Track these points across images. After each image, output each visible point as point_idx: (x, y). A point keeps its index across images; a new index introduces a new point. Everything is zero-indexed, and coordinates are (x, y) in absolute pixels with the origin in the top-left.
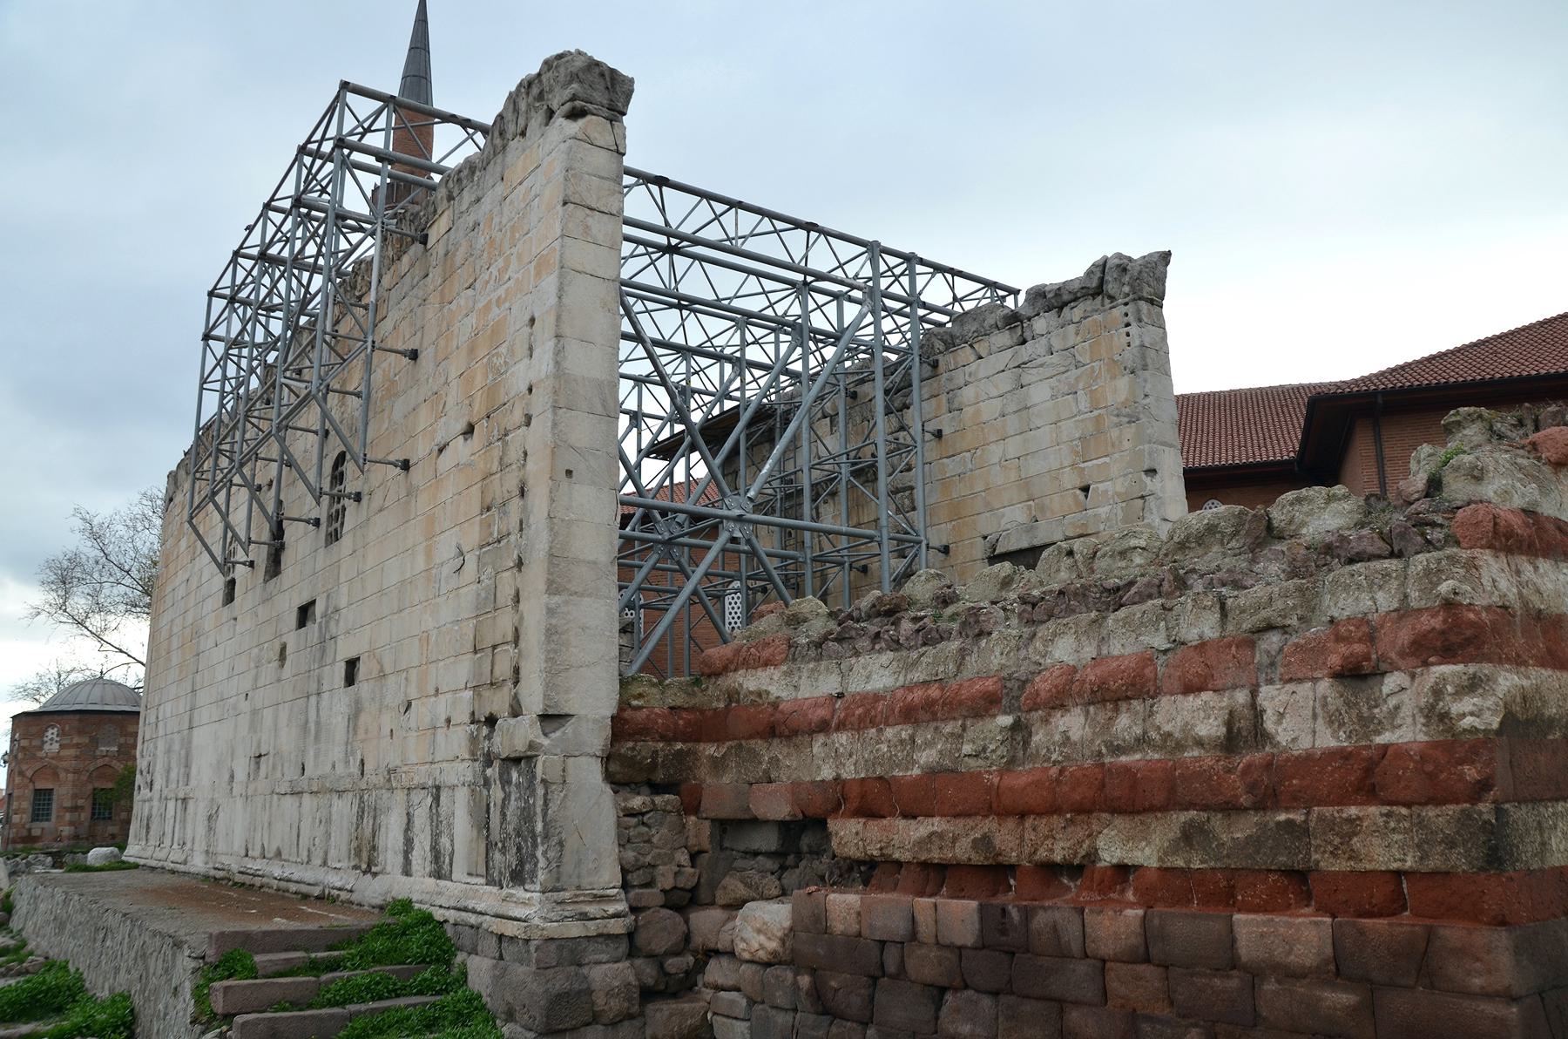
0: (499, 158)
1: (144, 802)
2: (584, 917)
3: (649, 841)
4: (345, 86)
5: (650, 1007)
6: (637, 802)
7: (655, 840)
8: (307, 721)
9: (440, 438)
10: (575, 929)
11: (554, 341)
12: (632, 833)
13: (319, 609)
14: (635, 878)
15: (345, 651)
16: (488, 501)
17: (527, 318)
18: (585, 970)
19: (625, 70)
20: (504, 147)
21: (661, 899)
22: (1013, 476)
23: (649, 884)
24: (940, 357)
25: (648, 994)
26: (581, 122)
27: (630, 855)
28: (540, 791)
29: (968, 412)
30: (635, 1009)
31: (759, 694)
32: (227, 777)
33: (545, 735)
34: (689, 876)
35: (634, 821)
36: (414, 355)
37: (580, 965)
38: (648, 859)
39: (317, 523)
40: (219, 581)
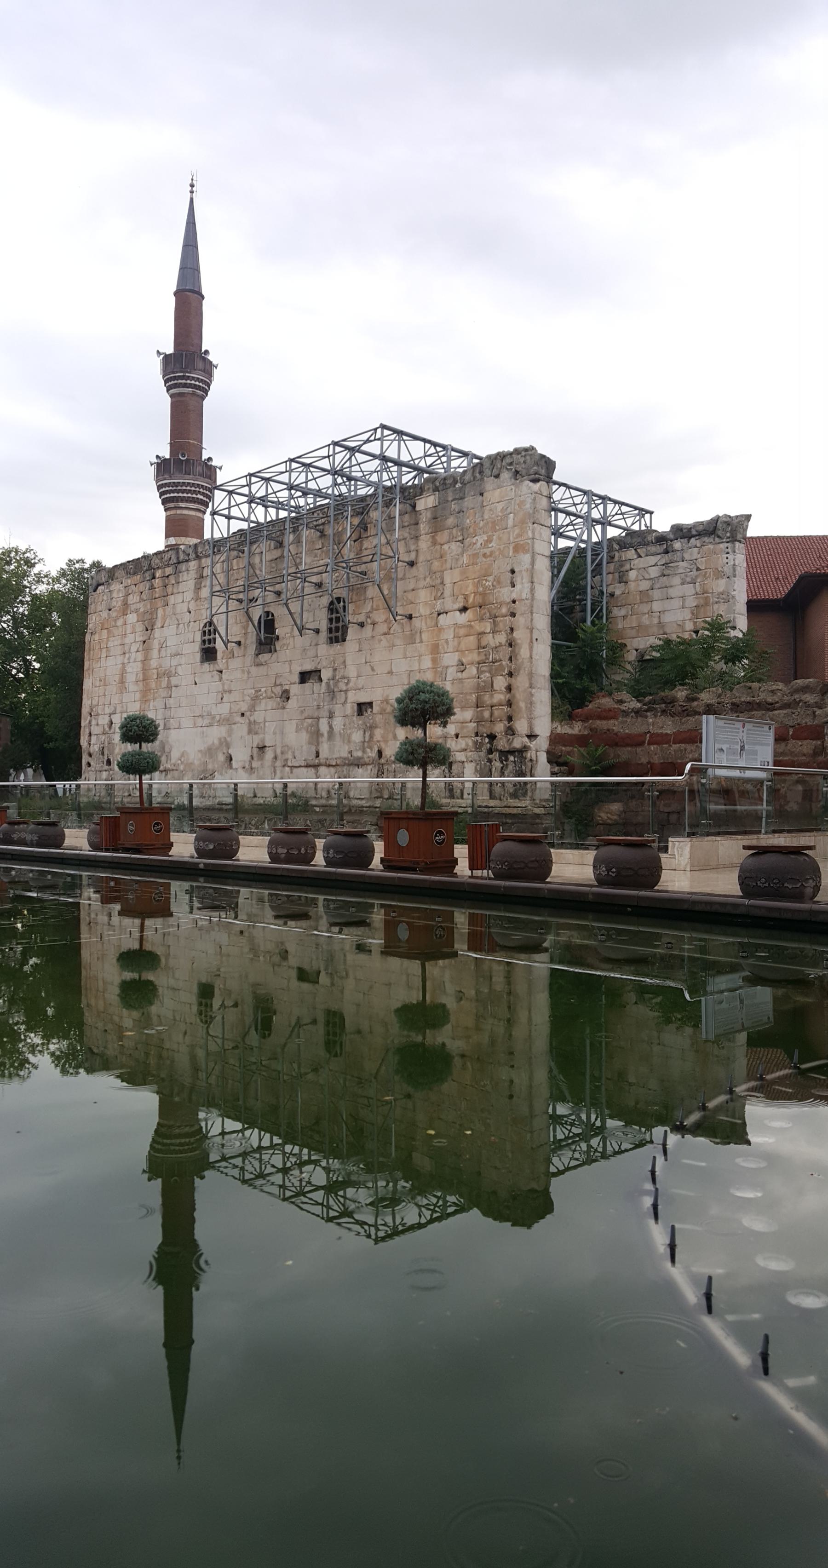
0: (477, 483)
4: (384, 427)
8: (318, 730)
9: (438, 607)
11: (530, 584)
13: (326, 675)
15: (355, 697)
16: (483, 644)
17: (509, 568)
19: (552, 458)
20: (482, 479)
22: (656, 621)
24: (617, 555)
26: (538, 484)
28: (529, 764)
29: (632, 586)
31: (608, 730)
32: (221, 758)
36: (412, 564)
39: (317, 631)
40: (194, 649)
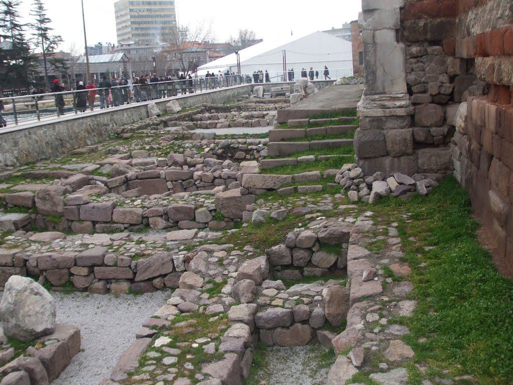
1: (91, 46)
2: (384, 107)
3: (423, 70)
5: (420, 152)
6: (414, 49)
7: (426, 70)
10: (379, 113)
12: (414, 66)
14: (414, 89)
18: (385, 132)
21: (430, 99)
23: (425, 92)
25: (418, 145)
27: (412, 77)
30: (410, 151)
33: (365, 20)
34: (447, 88)
35: (413, 60)
37: (383, 129)
38: (423, 79)
